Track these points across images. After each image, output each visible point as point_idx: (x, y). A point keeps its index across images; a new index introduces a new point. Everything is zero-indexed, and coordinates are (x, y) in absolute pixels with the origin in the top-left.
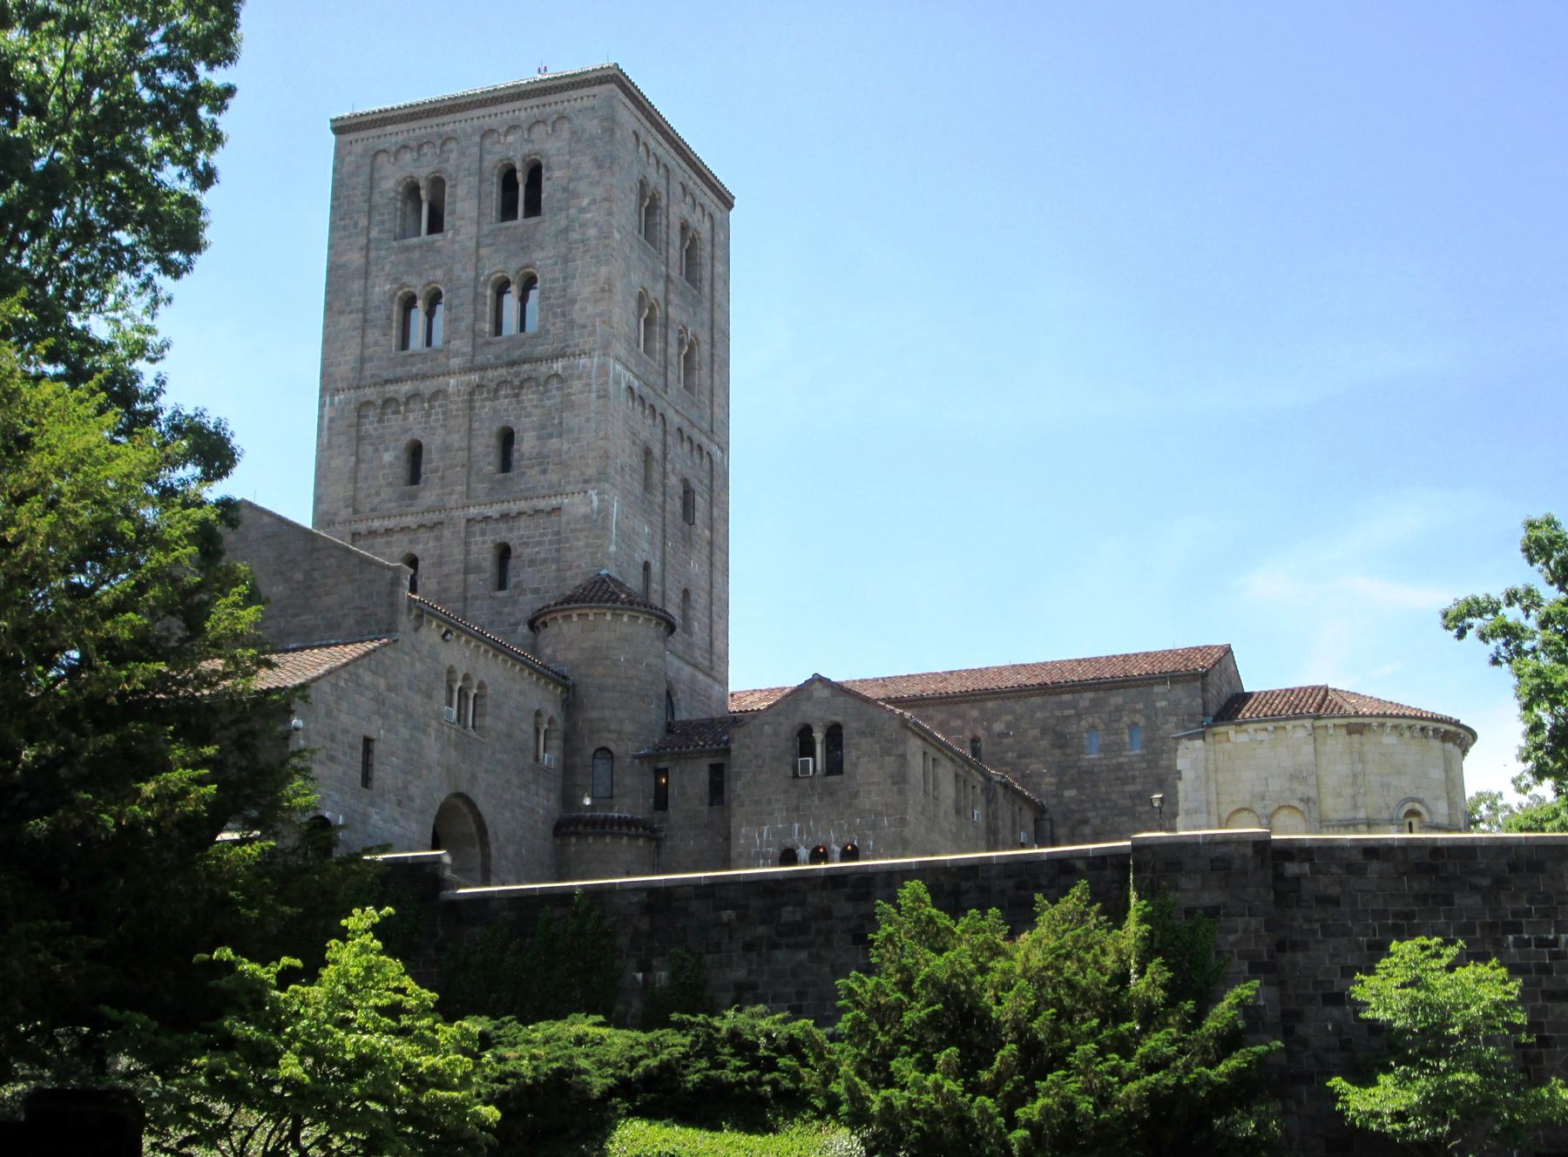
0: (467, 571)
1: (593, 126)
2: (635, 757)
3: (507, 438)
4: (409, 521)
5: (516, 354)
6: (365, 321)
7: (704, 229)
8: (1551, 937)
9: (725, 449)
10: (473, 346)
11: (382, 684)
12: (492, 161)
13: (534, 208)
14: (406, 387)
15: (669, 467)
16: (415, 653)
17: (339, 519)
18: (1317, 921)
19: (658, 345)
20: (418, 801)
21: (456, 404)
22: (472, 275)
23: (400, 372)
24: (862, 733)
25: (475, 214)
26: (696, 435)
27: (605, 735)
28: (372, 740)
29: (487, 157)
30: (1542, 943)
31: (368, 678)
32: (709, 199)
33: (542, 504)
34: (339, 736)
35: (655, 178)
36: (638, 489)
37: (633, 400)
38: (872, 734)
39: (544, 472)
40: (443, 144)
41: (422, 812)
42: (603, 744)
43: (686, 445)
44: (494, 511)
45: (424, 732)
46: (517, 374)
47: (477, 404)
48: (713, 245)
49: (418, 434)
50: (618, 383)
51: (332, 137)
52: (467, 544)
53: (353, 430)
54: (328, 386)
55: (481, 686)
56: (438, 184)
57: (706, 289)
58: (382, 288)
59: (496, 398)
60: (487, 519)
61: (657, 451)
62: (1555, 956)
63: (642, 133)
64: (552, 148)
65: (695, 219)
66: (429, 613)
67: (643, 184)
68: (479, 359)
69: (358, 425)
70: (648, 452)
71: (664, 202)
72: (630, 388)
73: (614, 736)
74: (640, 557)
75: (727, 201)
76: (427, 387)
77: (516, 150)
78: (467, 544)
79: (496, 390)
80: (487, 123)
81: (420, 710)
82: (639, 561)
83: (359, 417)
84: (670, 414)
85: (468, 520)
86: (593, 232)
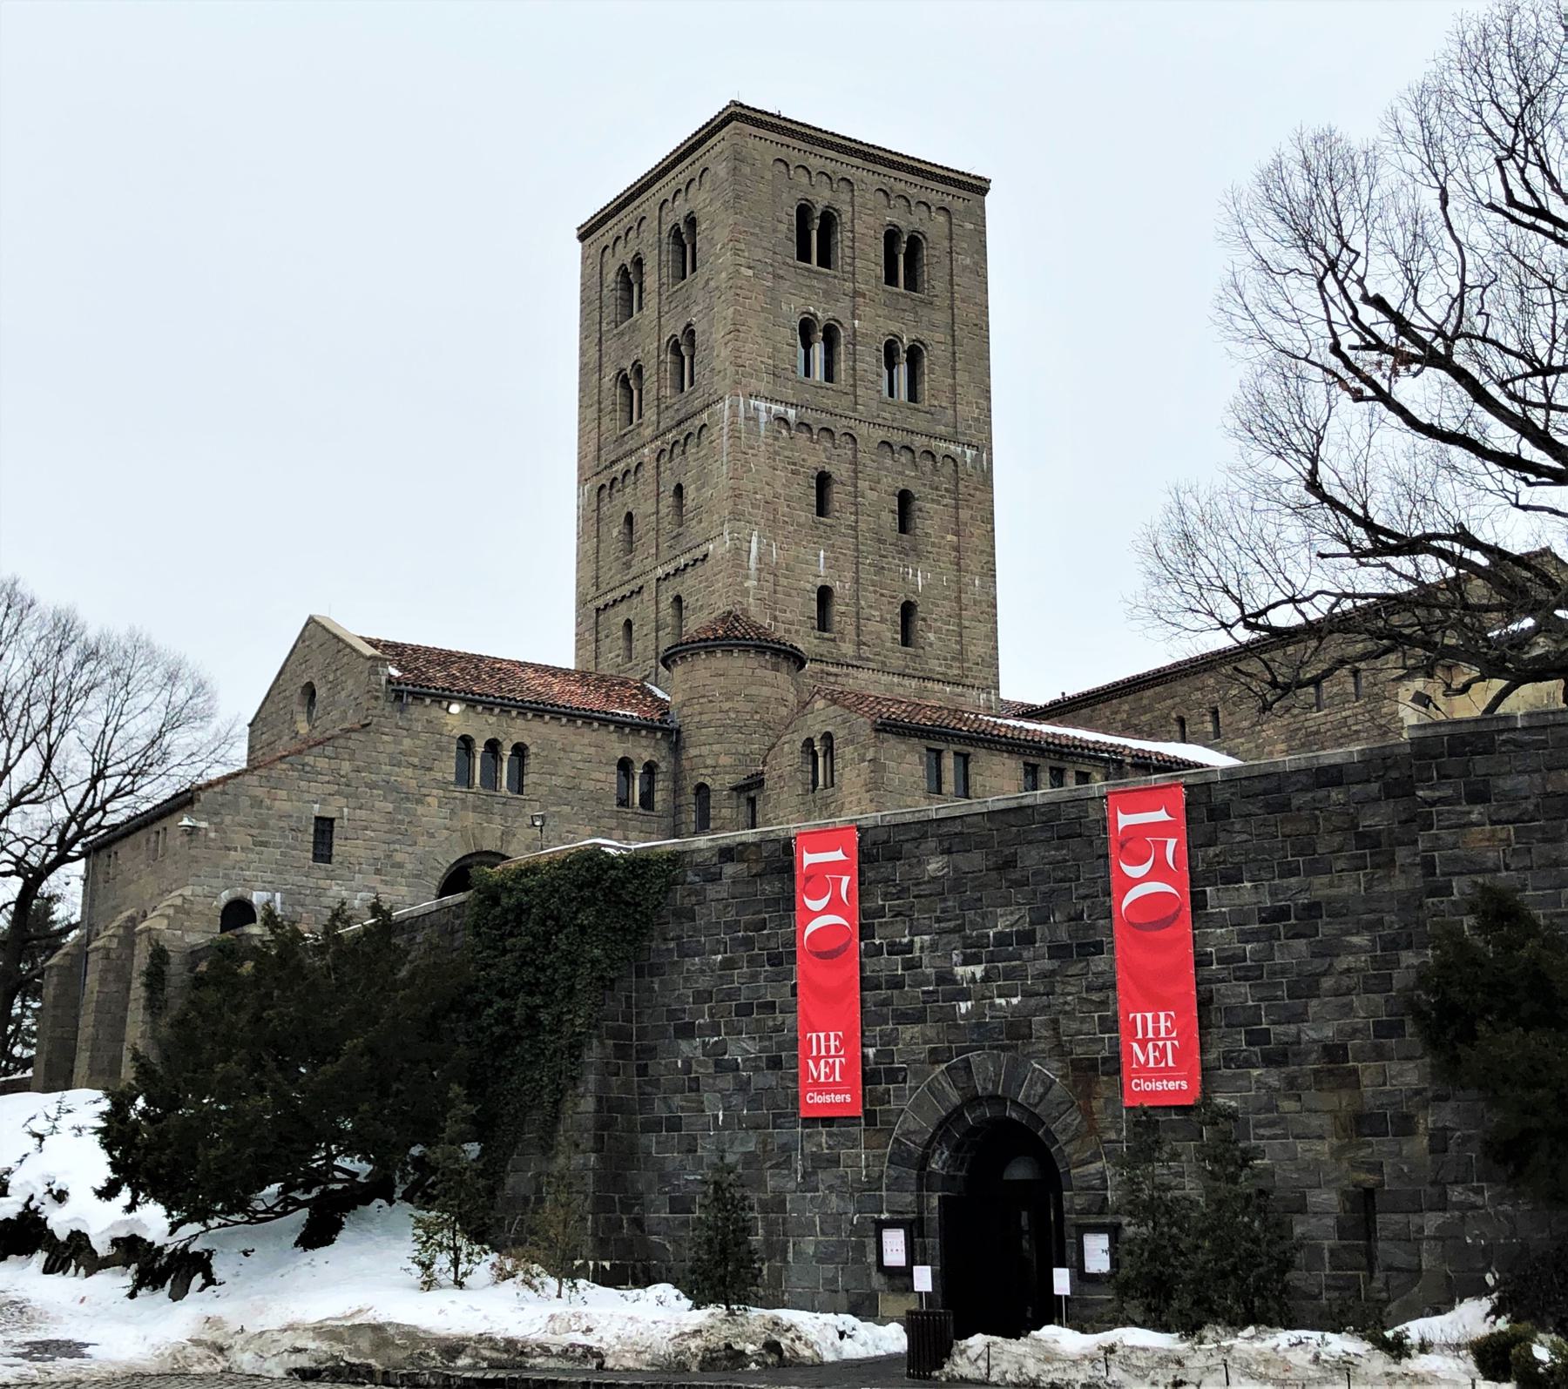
0: (657, 631)
1: (721, 170)
2: (733, 789)
3: (679, 490)
4: (625, 590)
5: (682, 415)
6: (600, 410)
7: (934, 227)
8: (905, 940)
9: (984, 446)
10: (658, 414)
11: (346, 767)
12: (666, 228)
13: (694, 269)
14: (621, 466)
15: (863, 485)
16: (405, 733)
17: (589, 598)
18: (672, 939)
19: (842, 366)
20: (409, 866)
21: (648, 472)
22: (656, 344)
23: (621, 451)
24: (847, 743)
25: (657, 285)
26: (919, 442)
27: (703, 771)
28: (332, 820)
29: (664, 227)
30: (895, 949)
31: (322, 764)
32: (936, 194)
33: (698, 554)
34: (272, 822)
35: (822, 198)
36: (806, 515)
37: (789, 429)
38: (852, 742)
39: (700, 521)
40: (639, 225)
41: (417, 876)
42: (701, 780)
43: (905, 458)
44: (670, 568)
45: (419, 802)
46: (681, 434)
47: (662, 469)
48: (951, 240)
49: (630, 507)
50: (752, 419)
51: (579, 245)
52: (657, 603)
53: (595, 514)
54: (582, 481)
55: (520, 750)
56: (638, 262)
57: (940, 286)
58: (610, 373)
59: (671, 459)
60: (668, 575)
61: (840, 471)
62: (910, 965)
63: (795, 157)
64: (699, 200)
65: (907, 222)
66: (410, 693)
67: (804, 212)
68: (663, 426)
69: (598, 508)
70: (823, 481)
71: (846, 218)
72: (783, 420)
73: (709, 771)
74: (810, 585)
75: (978, 187)
76: (632, 461)
77: (679, 212)
78: (657, 603)
79: (672, 451)
80: (660, 197)
81: (413, 783)
82: (809, 586)
83: (599, 501)
84: (863, 429)
85: (658, 580)
86: (724, 275)
